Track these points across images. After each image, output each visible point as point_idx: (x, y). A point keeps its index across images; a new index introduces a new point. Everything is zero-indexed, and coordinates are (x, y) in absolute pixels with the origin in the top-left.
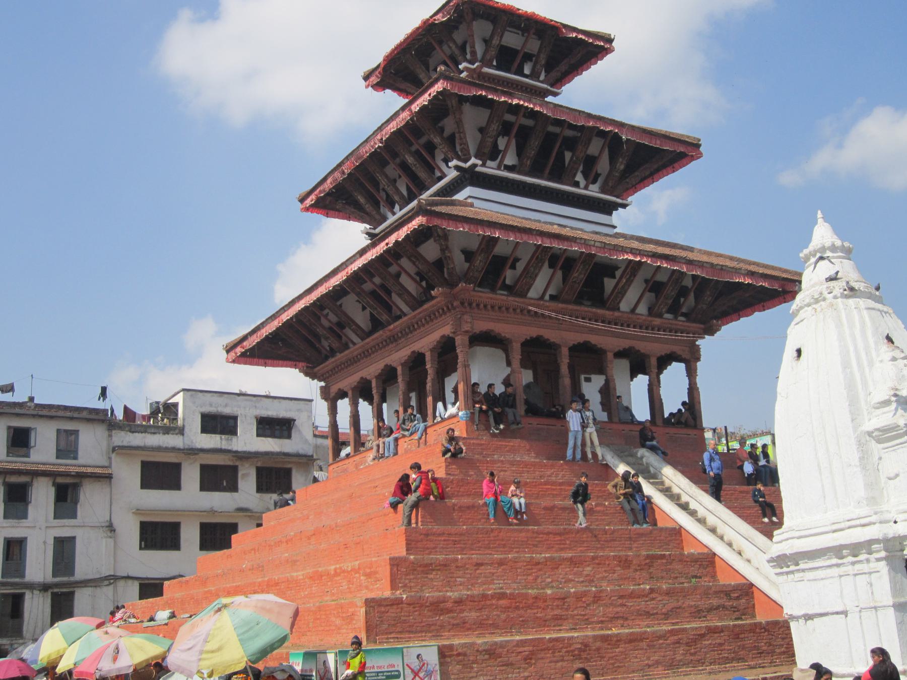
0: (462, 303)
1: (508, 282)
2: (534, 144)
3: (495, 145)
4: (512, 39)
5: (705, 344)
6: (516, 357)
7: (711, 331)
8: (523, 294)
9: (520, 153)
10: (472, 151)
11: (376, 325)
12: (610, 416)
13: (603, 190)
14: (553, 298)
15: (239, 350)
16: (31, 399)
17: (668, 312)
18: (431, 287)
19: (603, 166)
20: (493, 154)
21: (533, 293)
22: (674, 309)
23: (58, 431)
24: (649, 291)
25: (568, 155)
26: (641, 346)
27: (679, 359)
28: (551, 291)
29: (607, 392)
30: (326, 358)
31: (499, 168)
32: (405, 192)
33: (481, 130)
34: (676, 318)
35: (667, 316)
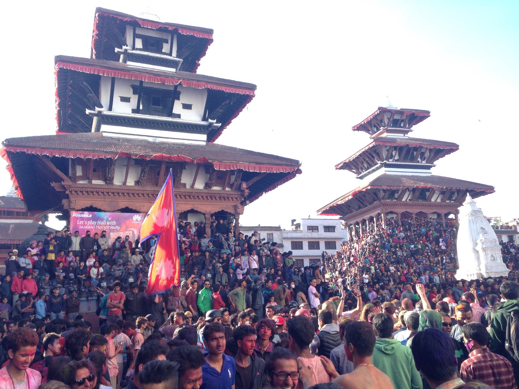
1: (396, 197)
2: (404, 152)
3: (392, 154)
4: (397, 117)
9: (399, 155)
10: (385, 157)
13: (427, 162)
16: (259, 225)
17: (448, 200)
19: (427, 154)
20: (392, 157)
21: (404, 200)
22: (450, 198)
23: (267, 234)
24: (442, 194)
25: (415, 153)
26: (439, 211)
28: (409, 198)
31: (393, 161)
32: (366, 166)
33: (387, 150)
34: (450, 202)
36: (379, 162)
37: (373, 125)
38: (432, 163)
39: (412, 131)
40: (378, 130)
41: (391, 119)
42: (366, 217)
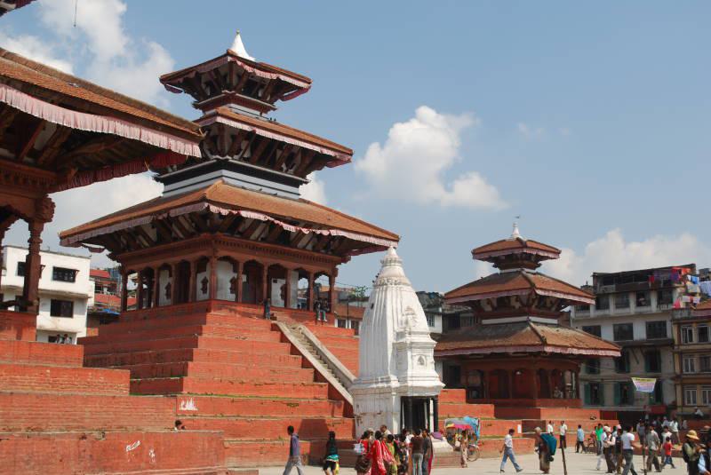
0: (216, 242)
3: (240, 147)
5: (341, 268)
6: (241, 270)
7: (345, 261)
8: (248, 238)
9: (252, 152)
10: (227, 149)
11: (161, 239)
12: (285, 305)
13: (295, 174)
14: (262, 239)
15: (72, 240)
18: (199, 230)
21: (252, 237)
25: (279, 153)
27: (326, 275)
28: (262, 236)
29: (285, 290)
30: (124, 250)
35: (323, 251)
36: (214, 157)
37: (203, 80)
38: (304, 177)
39: (274, 109)
40: (214, 92)
41: (245, 79)
42: (174, 260)
